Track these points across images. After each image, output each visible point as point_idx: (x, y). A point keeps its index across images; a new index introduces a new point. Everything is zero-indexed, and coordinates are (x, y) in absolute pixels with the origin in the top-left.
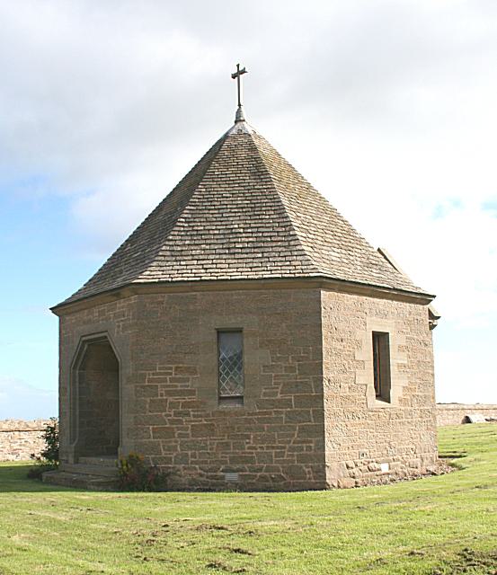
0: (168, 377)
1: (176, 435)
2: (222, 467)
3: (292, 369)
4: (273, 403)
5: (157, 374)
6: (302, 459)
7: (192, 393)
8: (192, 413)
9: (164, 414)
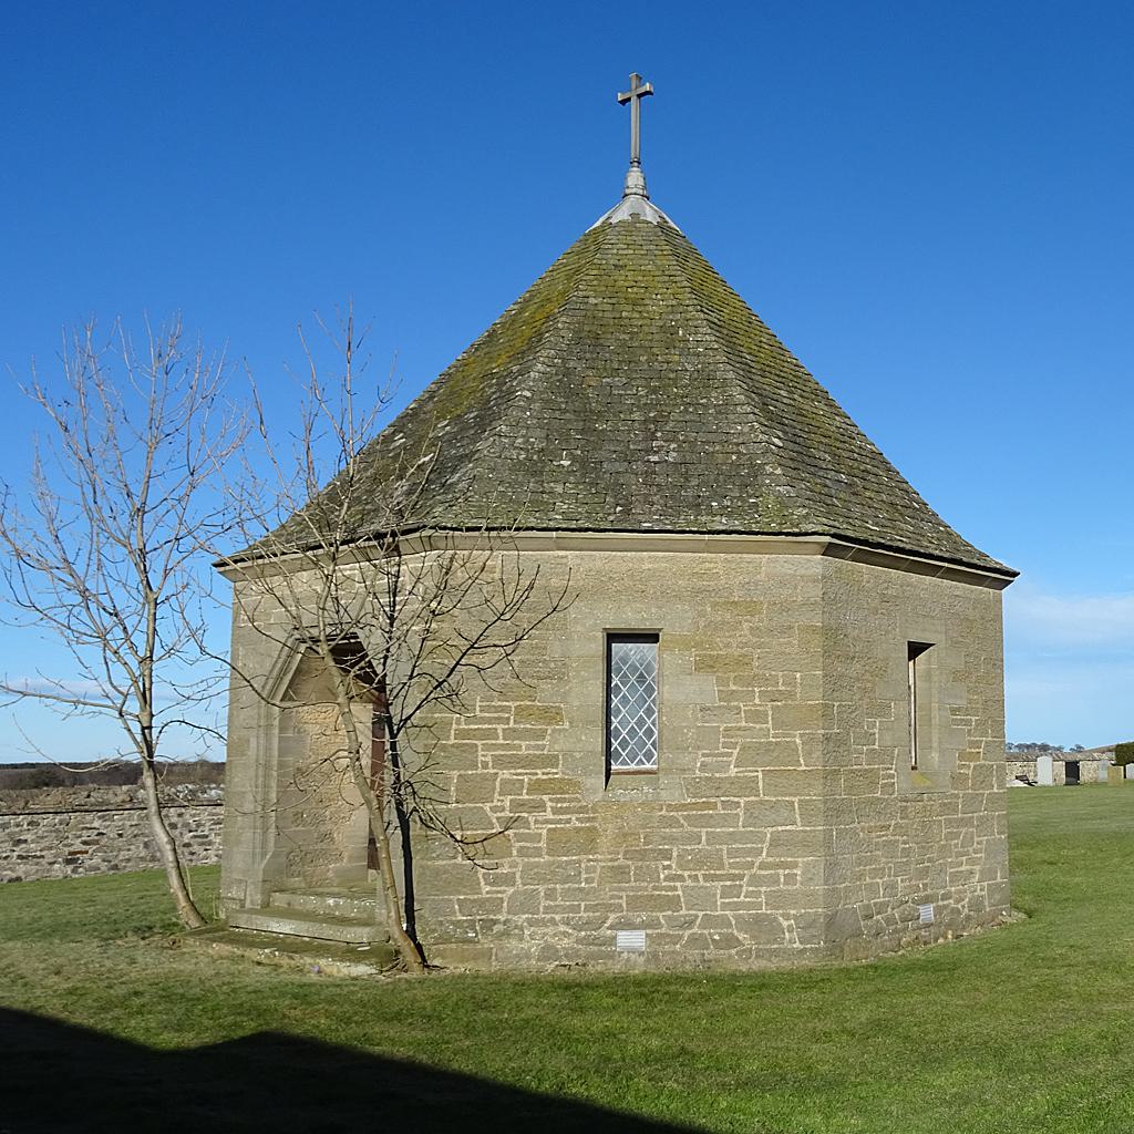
0: (500, 727)
1: (515, 853)
2: (612, 918)
3: (757, 716)
4: (718, 786)
5: (476, 720)
6: (777, 900)
7: (551, 761)
8: (549, 804)
9: (487, 807)
